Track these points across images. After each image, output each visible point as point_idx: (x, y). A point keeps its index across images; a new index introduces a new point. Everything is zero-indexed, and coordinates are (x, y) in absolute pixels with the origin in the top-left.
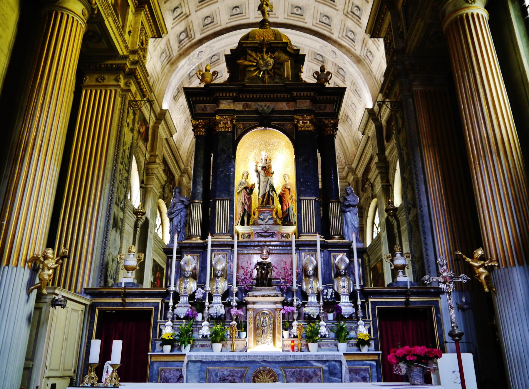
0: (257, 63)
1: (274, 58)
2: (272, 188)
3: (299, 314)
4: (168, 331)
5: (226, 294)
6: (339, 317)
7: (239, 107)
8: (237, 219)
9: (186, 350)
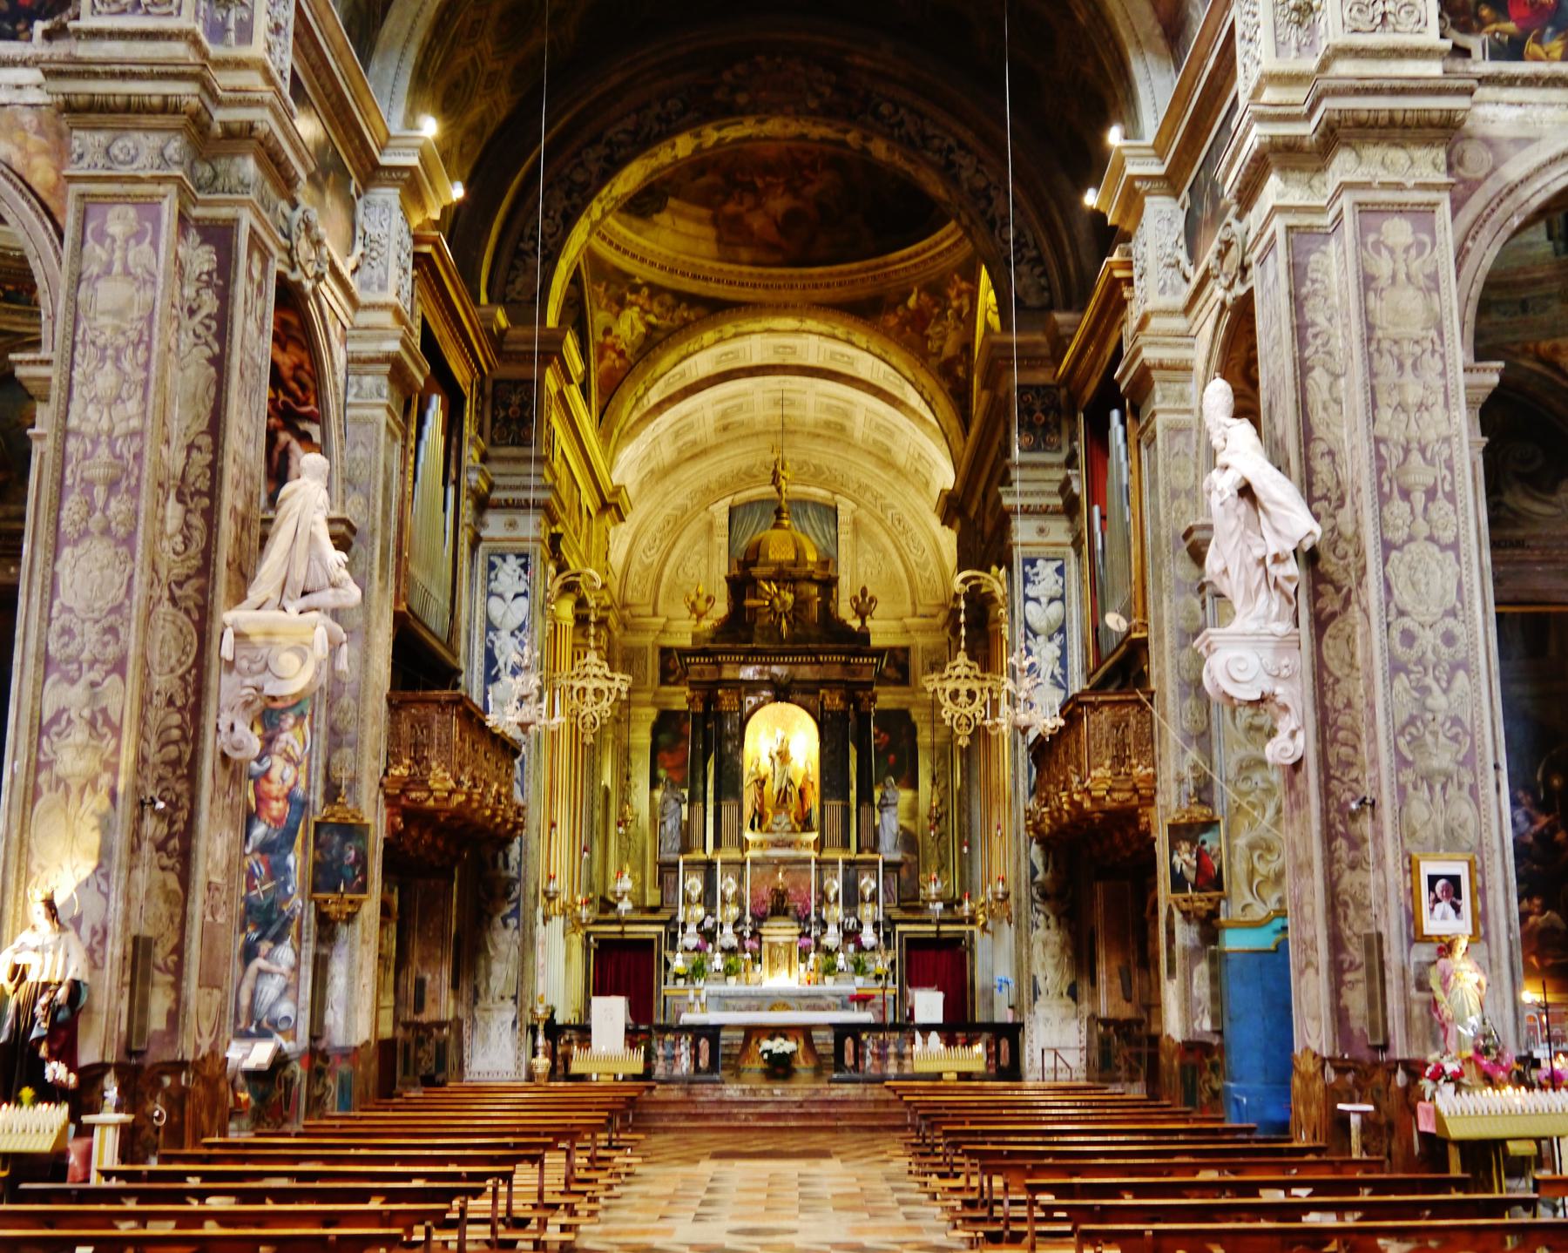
0: (771, 602)
1: (795, 593)
2: (791, 782)
4: (679, 963)
5: (737, 923)
6: (860, 948)
7: (749, 673)
8: (747, 823)
9: (700, 984)
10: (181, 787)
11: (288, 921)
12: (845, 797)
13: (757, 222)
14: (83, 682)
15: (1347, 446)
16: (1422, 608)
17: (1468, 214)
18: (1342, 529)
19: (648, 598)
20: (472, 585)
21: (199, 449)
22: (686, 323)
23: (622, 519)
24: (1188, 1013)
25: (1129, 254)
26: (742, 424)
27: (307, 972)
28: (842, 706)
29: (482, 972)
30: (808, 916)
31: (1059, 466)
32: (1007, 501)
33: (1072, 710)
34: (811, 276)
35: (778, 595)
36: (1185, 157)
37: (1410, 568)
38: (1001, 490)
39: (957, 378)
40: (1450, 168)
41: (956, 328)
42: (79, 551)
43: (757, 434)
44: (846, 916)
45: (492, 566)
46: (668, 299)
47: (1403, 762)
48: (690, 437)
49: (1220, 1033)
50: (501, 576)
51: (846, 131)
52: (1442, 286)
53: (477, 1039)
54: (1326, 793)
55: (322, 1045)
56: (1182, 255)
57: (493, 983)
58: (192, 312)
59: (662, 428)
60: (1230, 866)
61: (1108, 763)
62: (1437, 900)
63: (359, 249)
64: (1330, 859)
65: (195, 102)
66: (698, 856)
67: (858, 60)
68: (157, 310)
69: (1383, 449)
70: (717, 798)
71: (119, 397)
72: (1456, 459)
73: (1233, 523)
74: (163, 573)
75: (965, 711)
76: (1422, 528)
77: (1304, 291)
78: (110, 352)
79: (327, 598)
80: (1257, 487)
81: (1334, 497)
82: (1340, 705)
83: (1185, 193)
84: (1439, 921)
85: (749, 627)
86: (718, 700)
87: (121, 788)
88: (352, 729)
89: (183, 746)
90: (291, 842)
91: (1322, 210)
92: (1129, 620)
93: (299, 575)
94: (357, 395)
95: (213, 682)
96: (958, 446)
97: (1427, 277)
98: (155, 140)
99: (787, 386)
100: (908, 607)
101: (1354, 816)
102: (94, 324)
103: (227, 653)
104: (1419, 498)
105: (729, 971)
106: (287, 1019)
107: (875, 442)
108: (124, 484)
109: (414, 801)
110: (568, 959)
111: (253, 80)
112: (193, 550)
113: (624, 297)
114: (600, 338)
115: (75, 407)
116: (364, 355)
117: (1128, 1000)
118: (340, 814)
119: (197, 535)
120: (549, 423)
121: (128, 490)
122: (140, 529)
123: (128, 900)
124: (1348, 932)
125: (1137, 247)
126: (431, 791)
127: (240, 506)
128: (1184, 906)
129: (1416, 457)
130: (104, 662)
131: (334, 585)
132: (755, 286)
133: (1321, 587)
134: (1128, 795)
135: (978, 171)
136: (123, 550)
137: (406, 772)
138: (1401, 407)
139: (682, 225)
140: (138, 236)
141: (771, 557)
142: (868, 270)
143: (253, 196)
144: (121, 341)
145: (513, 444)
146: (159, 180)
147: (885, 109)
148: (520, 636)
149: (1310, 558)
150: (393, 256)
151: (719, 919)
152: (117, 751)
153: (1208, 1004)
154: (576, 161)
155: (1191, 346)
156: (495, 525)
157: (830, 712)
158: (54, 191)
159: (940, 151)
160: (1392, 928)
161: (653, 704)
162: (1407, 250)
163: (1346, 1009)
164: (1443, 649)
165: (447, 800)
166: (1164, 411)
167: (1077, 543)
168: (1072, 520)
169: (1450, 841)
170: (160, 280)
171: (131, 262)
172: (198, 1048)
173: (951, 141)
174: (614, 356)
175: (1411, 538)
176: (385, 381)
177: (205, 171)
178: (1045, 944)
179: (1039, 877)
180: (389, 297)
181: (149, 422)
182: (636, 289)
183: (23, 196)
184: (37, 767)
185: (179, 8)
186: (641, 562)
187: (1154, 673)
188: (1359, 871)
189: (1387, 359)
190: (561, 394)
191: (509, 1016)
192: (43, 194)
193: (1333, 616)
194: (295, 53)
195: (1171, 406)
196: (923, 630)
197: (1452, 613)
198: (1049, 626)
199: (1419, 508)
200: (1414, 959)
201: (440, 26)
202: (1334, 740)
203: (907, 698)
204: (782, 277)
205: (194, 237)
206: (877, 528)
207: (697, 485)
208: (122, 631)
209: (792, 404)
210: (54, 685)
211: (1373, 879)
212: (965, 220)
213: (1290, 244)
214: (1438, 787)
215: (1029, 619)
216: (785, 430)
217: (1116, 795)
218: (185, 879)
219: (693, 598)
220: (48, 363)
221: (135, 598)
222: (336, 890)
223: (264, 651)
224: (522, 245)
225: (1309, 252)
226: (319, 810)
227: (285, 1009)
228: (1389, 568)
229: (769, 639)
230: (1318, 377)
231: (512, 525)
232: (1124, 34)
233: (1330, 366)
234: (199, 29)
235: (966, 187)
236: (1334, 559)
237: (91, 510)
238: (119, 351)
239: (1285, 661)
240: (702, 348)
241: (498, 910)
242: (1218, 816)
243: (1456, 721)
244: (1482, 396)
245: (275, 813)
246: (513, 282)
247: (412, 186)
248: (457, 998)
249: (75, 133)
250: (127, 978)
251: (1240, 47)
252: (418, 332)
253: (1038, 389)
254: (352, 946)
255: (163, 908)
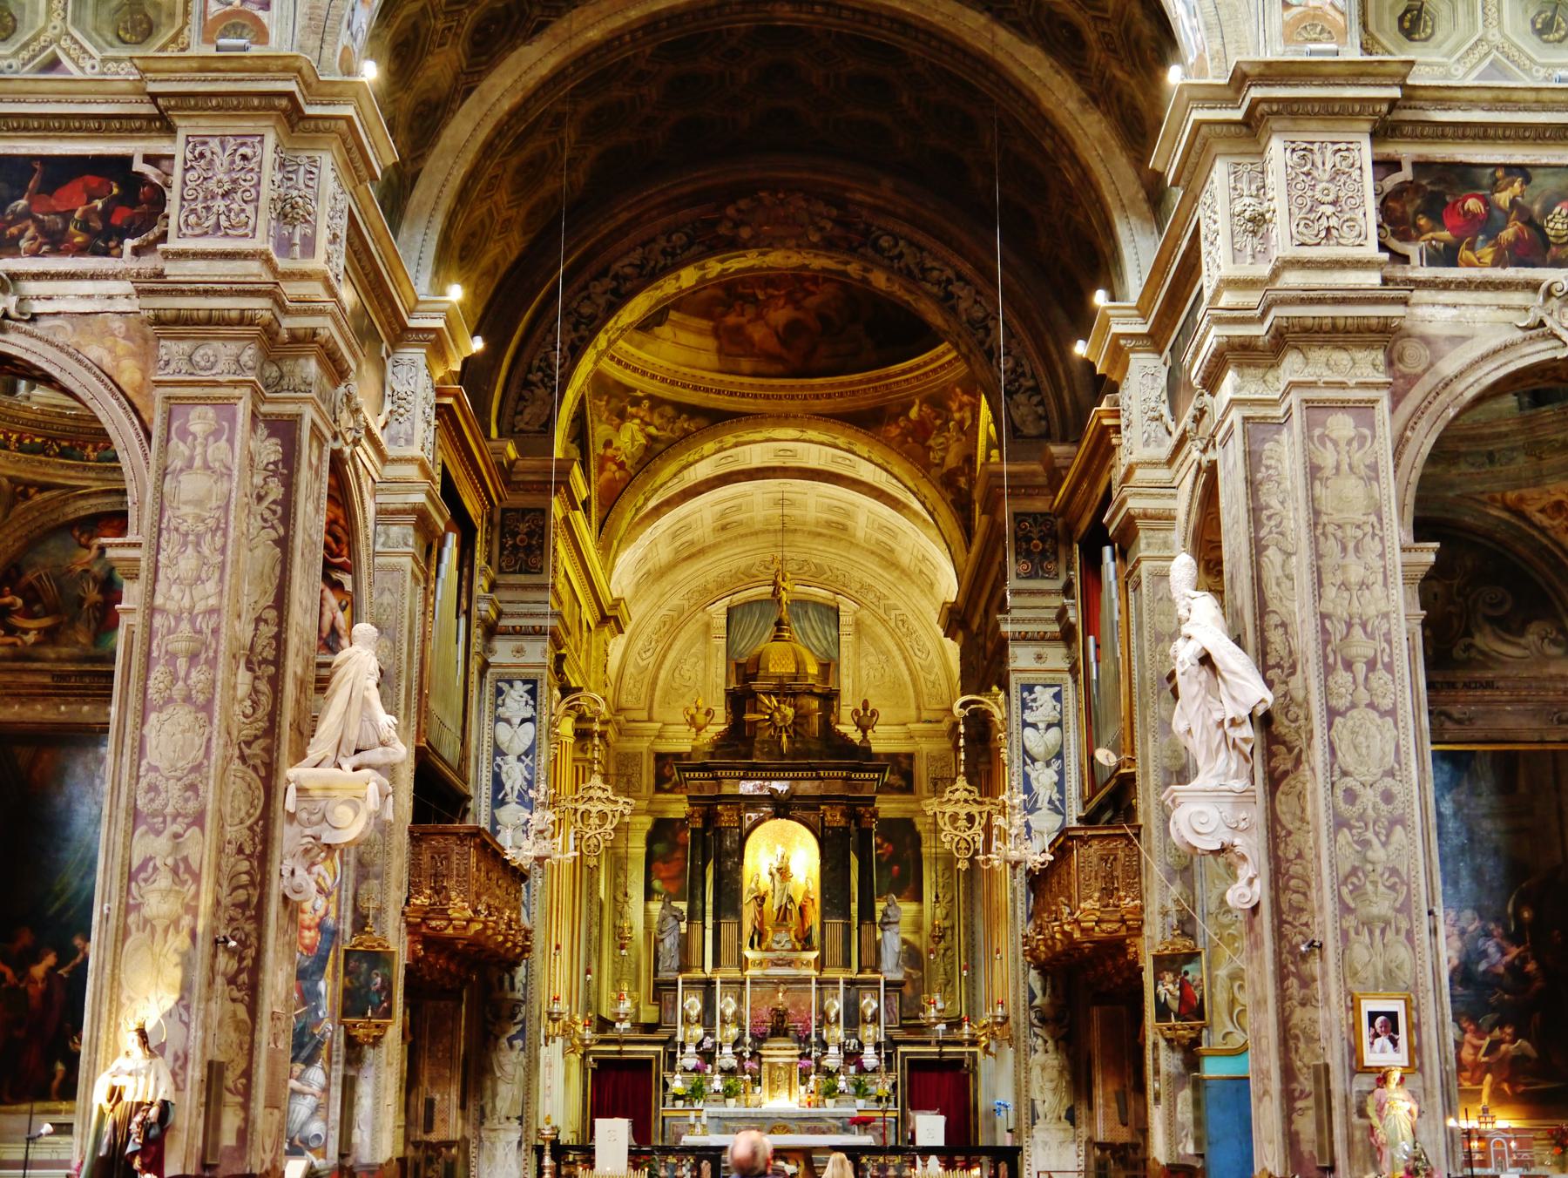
1: (795, 706)
2: (791, 899)
3: (818, 1066)
4: (678, 1084)
5: (736, 1043)
6: (862, 1070)
7: (747, 788)
8: (746, 941)
10: (249, 927)
11: (317, 1047)
12: (847, 915)
13: (758, 333)
14: (167, 833)
15: (1298, 620)
16: (1363, 769)
17: (1407, 407)
18: (1294, 694)
19: (643, 703)
20: (480, 711)
21: (266, 621)
22: (687, 434)
23: (621, 631)
24: (1172, 1138)
25: (1116, 403)
26: (740, 523)
27: (336, 1092)
28: (843, 823)
29: (489, 1093)
30: (809, 1036)
31: (1056, 593)
32: (1006, 628)
33: (1063, 846)
34: (812, 387)
35: (778, 709)
36: (1166, 321)
37: (1353, 732)
38: (999, 617)
39: (959, 489)
40: (1390, 363)
41: (959, 440)
42: (164, 716)
43: (756, 533)
44: (847, 1037)
45: (500, 692)
46: (669, 411)
47: (1346, 909)
48: (688, 537)
49: (1202, 1156)
50: (508, 701)
51: (847, 263)
52: (1382, 475)
53: (483, 1157)
54: (1279, 936)
55: (349, 1162)
56: (1165, 409)
57: (499, 1104)
58: (260, 498)
59: (660, 530)
60: (1211, 996)
61: (1097, 895)
62: (1377, 1035)
63: (388, 407)
64: (1282, 997)
65: (268, 315)
66: (697, 974)
67: (859, 197)
68: (233, 500)
69: (1328, 624)
70: (716, 916)
71: (199, 578)
72: (1394, 633)
73: (1195, 688)
74: (235, 733)
75: (964, 835)
76: (1363, 696)
77: (1259, 476)
78: (191, 538)
79: (376, 756)
80: (1215, 657)
81: (1286, 665)
82: (1292, 856)
83: (1167, 352)
84: (1378, 1053)
85: (749, 741)
86: (718, 815)
87: (200, 929)
88: (378, 861)
89: (251, 891)
90: (323, 969)
91: (1274, 403)
92: (1118, 756)
93: (353, 736)
94: (384, 545)
95: (277, 833)
96: (961, 559)
97: (1367, 466)
98: (233, 348)
99: (787, 488)
100: (913, 713)
101: (1304, 957)
102: (178, 513)
103: (290, 805)
104: (1360, 668)
105: (729, 1092)
106: (318, 1137)
107: (878, 542)
108: (203, 656)
109: (434, 929)
110: (567, 1079)
111: (315, 290)
112: (260, 713)
113: (625, 408)
114: (600, 451)
115: (161, 587)
116: (391, 507)
117: (1125, 1124)
118: (366, 943)
119: (263, 698)
120: (555, 550)
121: (207, 661)
122: (218, 696)
123: (205, 1030)
124: (1299, 1064)
125: (1123, 396)
126: (450, 920)
127: (299, 671)
128: (1169, 1034)
129: (1357, 631)
130: (185, 816)
131: (383, 744)
132: (755, 396)
133: (1274, 748)
134: (1116, 926)
135: (976, 302)
136: (202, 715)
137: (427, 902)
138: (1344, 585)
139: (684, 337)
140: (216, 434)
141: (772, 670)
142: (870, 381)
143: (314, 394)
144: (201, 528)
145: (521, 572)
146: (235, 384)
147: (885, 242)
148: (527, 761)
149: (1264, 721)
150: (419, 412)
151: (718, 1039)
152: (197, 895)
153: (1191, 1129)
154: (584, 294)
155: (1174, 496)
156: (503, 651)
157: (832, 828)
158: (139, 390)
159: (939, 283)
160: (1335, 1058)
161: (648, 812)
162: (1349, 443)
163: (1297, 1133)
164: (1382, 806)
165: (465, 928)
166: (1148, 558)
167: (1073, 670)
168: (1069, 647)
169: (1389, 981)
170: (236, 473)
171: (210, 458)
172: (263, 1162)
173: (949, 273)
174: (614, 468)
175: (1353, 706)
176: (410, 530)
177: (273, 372)
178: (1043, 1069)
179: (1037, 1002)
180: (415, 451)
181: (225, 601)
182: (636, 402)
183: (113, 395)
184: (128, 909)
185: (254, 230)
186: (637, 665)
187: (1141, 808)
188: (1309, 1007)
189: (1332, 541)
190: (566, 520)
191: (515, 1137)
192: (129, 392)
193: (1286, 774)
194: (348, 257)
195: (1156, 554)
196: (927, 736)
197: (1391, 773)
198: (1048, 752)
199: (1361, 678)
200: (1355, 1088)
201: (463, 195)
202: (1287, 888)
203: (912, 806)
204: (783, 387)
205: (262, 430)
206: (880, 630)
207: (694, 584)
208: (201, 787)
209: (793, 504)
210: (142, 835)
211: (1321, 1014)
212: (964, 349)
213: (1246, 433)
214: (1377, 932)
215: (1027, 744)
216: (785, 529)
217: (1104, 926)
218: (253, 1010)
219: (693, 711)
220: (137, 545)
221: (213, 758)
222: (364, 1015)
223: (322, 804)
224: (530, 377)
225: (1264, 441)
226: (348, 941)
227: (316, 1127)
228: (1333, 733)
229: (770, 754)
230: (1272, 555)
231: (519, 651)
232: (1109, 199)
233: (1283, 545)
234: (270, 247)
235: (964, 318)
236: (1286, 722)
237: (175, 680)
238: (199, 536)
239: (1243, 815)
240: (702, 458)
241: (505, 1032)
242: (1200, 948)
243: (1394, 872)
244: (1421, 572)
245: (307, 941)
246: (521, 413)
247: (436, 344)
248: (465, 1118)
249: (162, 342)
250: (203, 1099)
251: (1204, 247)
252: (438, 479)
253: (1034, 516)
254: (378, 1068)
255: (233, 1036)
